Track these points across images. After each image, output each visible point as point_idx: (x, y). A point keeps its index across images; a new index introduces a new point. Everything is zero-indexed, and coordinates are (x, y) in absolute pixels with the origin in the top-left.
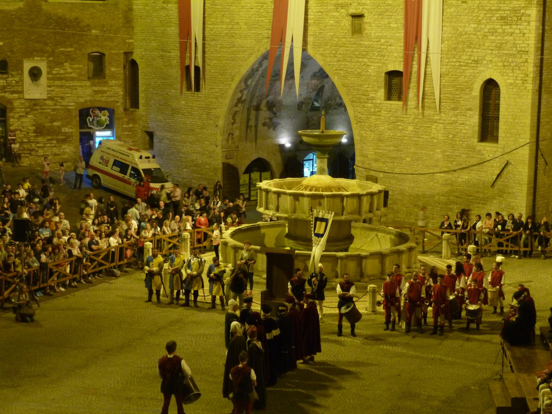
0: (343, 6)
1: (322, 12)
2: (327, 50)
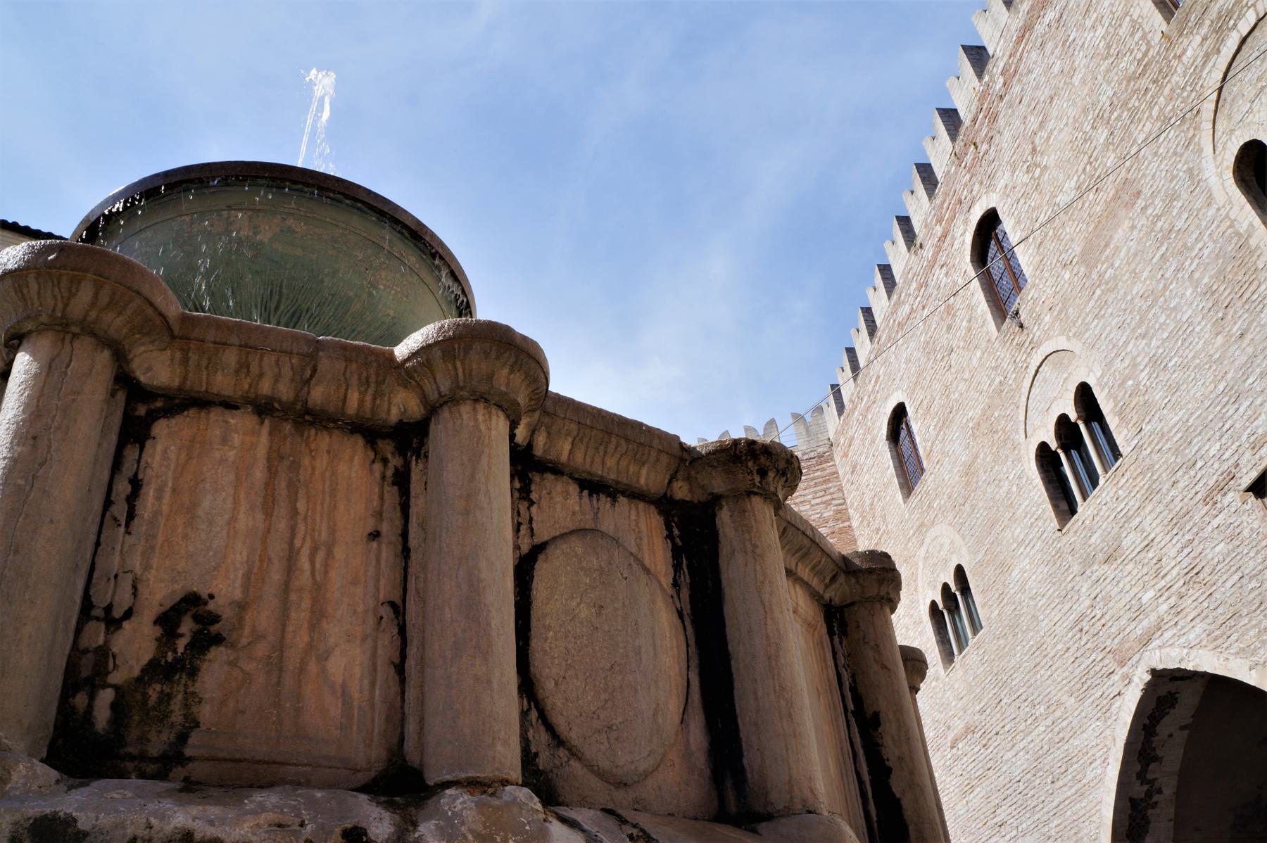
0: (1221, 488)
1: (1191, 541)
2: (1248, 630)
